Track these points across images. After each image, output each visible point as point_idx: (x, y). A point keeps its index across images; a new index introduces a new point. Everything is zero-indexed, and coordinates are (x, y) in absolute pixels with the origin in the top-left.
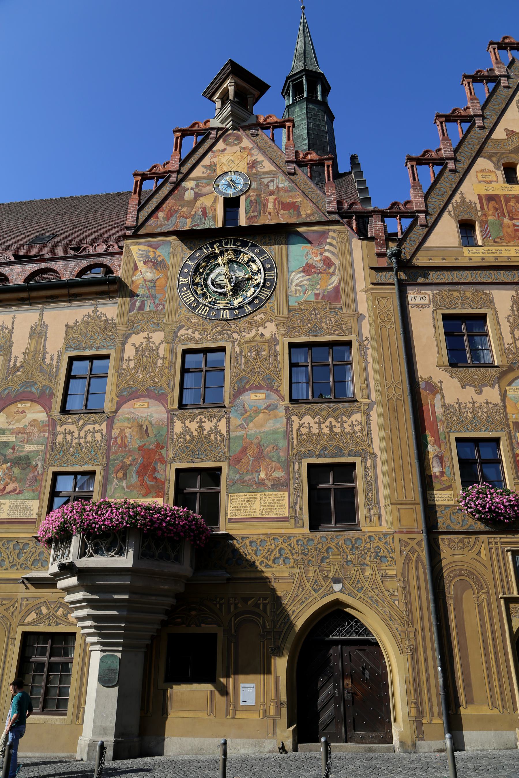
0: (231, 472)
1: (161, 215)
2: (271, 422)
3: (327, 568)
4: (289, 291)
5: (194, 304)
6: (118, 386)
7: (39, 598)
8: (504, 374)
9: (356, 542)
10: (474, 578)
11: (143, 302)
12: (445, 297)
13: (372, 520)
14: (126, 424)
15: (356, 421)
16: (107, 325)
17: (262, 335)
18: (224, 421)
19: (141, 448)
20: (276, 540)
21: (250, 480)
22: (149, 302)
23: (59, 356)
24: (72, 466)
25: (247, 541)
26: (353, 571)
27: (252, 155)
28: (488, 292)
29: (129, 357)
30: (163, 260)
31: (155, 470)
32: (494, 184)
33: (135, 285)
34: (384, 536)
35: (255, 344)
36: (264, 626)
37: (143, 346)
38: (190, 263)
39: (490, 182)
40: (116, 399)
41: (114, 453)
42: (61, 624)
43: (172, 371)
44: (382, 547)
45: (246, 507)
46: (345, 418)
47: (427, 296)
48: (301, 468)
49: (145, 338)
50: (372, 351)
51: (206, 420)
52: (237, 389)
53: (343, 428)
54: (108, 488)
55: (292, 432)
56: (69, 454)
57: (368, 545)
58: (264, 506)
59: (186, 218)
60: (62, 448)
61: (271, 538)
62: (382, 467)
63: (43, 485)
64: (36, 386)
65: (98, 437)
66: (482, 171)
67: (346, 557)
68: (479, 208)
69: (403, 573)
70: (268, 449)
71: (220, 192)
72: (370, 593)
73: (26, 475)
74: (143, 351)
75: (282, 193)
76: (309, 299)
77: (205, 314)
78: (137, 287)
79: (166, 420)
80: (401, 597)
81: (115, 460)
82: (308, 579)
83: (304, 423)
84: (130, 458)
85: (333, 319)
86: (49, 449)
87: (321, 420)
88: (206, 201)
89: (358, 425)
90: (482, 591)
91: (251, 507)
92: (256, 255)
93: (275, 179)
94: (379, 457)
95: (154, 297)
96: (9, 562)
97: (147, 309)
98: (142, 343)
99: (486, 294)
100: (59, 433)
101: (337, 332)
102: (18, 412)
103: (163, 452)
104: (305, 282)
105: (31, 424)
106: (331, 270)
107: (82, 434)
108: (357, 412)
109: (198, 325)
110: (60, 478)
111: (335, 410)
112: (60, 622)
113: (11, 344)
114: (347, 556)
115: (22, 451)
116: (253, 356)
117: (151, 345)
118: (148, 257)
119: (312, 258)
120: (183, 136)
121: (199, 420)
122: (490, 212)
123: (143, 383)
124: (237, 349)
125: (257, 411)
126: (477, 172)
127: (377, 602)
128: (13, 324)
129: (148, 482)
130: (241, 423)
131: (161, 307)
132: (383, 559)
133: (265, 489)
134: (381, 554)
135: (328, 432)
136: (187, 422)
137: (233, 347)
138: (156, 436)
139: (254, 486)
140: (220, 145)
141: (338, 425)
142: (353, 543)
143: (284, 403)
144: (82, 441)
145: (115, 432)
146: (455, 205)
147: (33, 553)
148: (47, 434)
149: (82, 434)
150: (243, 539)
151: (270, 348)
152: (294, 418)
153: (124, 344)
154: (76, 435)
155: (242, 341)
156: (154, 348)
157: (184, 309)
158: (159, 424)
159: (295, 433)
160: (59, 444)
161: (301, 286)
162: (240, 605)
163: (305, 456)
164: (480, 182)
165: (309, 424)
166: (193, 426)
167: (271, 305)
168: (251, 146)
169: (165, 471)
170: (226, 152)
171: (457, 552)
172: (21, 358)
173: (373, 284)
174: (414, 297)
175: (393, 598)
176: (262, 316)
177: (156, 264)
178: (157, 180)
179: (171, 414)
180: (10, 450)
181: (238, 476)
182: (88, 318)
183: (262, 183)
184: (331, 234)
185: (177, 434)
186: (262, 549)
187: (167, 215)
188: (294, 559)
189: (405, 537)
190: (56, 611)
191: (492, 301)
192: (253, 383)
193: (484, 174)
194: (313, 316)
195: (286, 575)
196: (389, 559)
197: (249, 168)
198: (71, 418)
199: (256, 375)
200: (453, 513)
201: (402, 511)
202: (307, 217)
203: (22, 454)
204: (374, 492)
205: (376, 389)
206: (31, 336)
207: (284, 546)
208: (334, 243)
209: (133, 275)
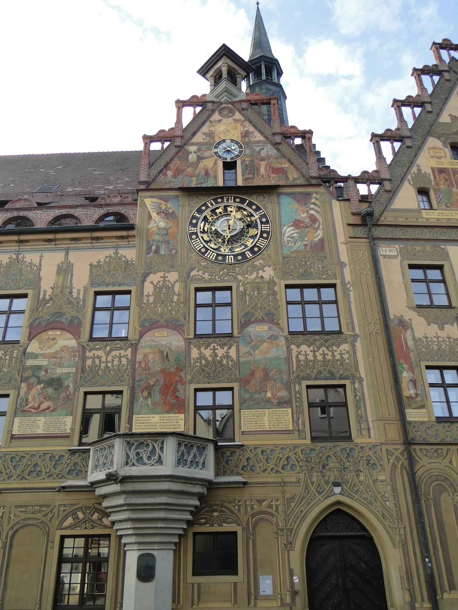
0: (242, 392)
1: (169, 173)
2: (274, 350)
3: (328, 473)
4: (283, 241)
5: (203, 250)
6: (140, 318)
7: (75, 504)
9: (350, 451)
10: (448, 482)
11: (158, 247)
12: (410, 250)
13: (363, 433)
14: (148, 350)
15: (344, 350)
17: (262, 277)
18: (234, 348)
19: (162, 371)
20: (283, 449)
21: (258, 398)
22: (163, 247)
23: (85, 291)
24: (101, 386)
25: (259, 451)
26: (349, 476)
27: (244, 126)
28: (443, 247)
29: (148, 293)
30: (174, 211)
31: (176, 390)
32: (443, 160)
33: (150, 232)
34: (373, 446)
36: (277, 525)
37: (161, 284)
38: (197, 215)
39: (440, 158)
41: (138, 375)
42: (96, 527)
43: (187, 306)
44: (372, 456)
45: (257, 421)
46: (335, 348)
47: (395, 249)
48: (301, 389)
49: (162, 277)
50: (354, 293)
51: (219, 347)
52: (243, 322)
53: (334, 356)
54: (135, 405)
55: (292, 358)
56: (98, 376)
57: (361, 454)
58: (272, 421)
59: (192, 177)
60: (91, 371)
61: (279, 448)
62: (368, 389)
63: (75, 403)
64: (65, 317)
65: (124, 361)
66: (434, 148)
67: (342, 464)
68: (432, 178)
69: (391, 478)
70: (273, 372)
71: (220, 157)
72: (365, 495)
73: (59, 395)
74: (161, 288)
75: (271, 160)
76: (299, 249)
77: (213, 259)
78: (152, 233)
79: (184, 347)
80: (391, 498)
81: (140, 381)
82: (312, 483)
83: (301, 351)
84: (153, 380)
85: (320, 266)
86: (80, 371)
87: (316, 349)
88: (209, 163)
89: (346, 353)
90: (456, 494)
91: (260, 421)
92: (253, 210)
93: (265, 147)
94: (365, 380)
95: (168, 243)
96: (46, 473)
97: (162, 253)
98: (159, 282)
99: (442, 249)
100: (88, 358)
101: (324, 276)
102: (49, 339)
103: (183, 374)
105: (62, 350)
106: (316, 225)
107: (110, 358)
108: (345, 343)
109: (208, 268)
110: (89, 397)
111: (326, 341)
112: (95, 525)
113: (40, 279)
114: (344, 463)
115: (54, 374)
116: (256, 294)
117: (168, 283)
118: (160, 208)
119: (300, 215)
120: (183, 106)
121: (212, 348)
122: (442, 182)
123: (162, 315)
124: (241, 289)
125: (262, 341)
126: (429, 149)
127: (371, 503)
128: (40, 262)
129: (170, 400)
130: (248, 350)
131: (174, 251)
132: (374, 466)
133: (272, 406)
134: (372, 462)
135: (322, 359)
136: (202, 349)
137: (238, 287)
138: (175, 360)
139: (262, 404)
140: (216, 116)
141: (330, 353)
142: (348, 452)
143: (284, 334)
144: (109, 365)
145: (139, 357)
146: (413, 175)
147: (68, 464)
149: (110, 358)
150: (255, 449)
151: (269, 289)
152: (293, 347)
153: (143, 282)
154: (104, 359)
155: (246, 282)
156: (170, 286)
157: (195, 254)
158: (178, 351)
159: (294, 359)
160: (89, 367)
161: (292, 238)
162: (255, 506)
163: (304, 378)
164: (432, 157)
165: (306, 352)
166: (207, 353)
167: (268, 253)
168: (243, 119)
169: (185, 390)
170: (222, 122)
171: (433, 461)
172: (49, 292)
173: (350, 237)
174: (384, 250)
175: (385, 499)
176: (261, 261)
177: (167, 215)
178: (163, 144)
179: (188, 341)
180: (43, 373)
181: (248, 395)
182: (110, 259)
183: (254, 150)
184: (314, 195)
185: (194, 359)
186: (272, 457)
187: (174, 174)
188: (301, 466)
189: (391, 448)
190: (92, 516)
191: (447, 255)
193: (435, 151)
194: (303, 263)
195: (294, 480)
196: (379, 466)
197: (242, 137)
198: (99, 345)
199: (259, 311)
200: (428, 428)
201: (386, 425)
202: (293, 181)
203: (55, 376)
204: (363, 409)
205: (359, 325)
206: (58, 273)
207: (291, 454)
208: (318, 203)
209: (148, 223)
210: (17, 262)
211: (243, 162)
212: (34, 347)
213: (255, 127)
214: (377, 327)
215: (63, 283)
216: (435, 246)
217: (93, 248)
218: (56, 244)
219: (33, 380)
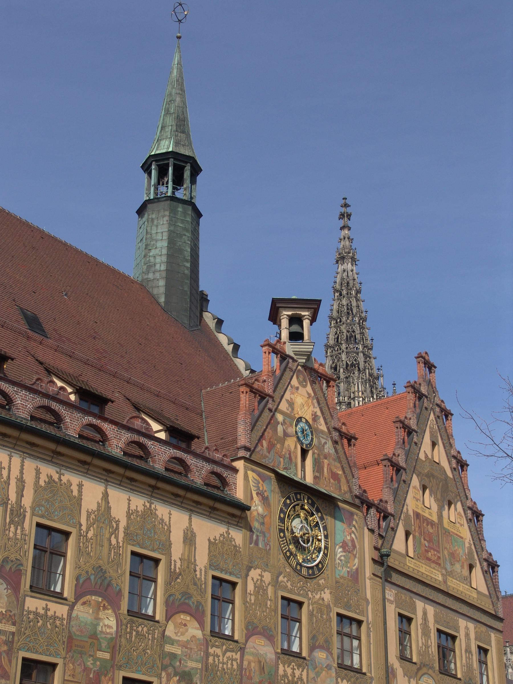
6: (245, 619)
8: (419, 669)
17: (323, 599)
35: (319, 607)
40: (245, 631)
59: (280, 457)
86: (204, 669)
97: (260, 546)
104: (342, 558)
124: (311, 608)
125: (322, 669)
128: (170, 521)
144: (225, 666)
145: (245, 663)
148: (202, 653)
149: (225, 660)
153: (247, 575)
154: (221, 658)
168: (313, 395)
177: (265, 500)
180: (178, 663)
184: (355, 517)
192: (320, 643)
198: (218, 642)
203: (187, 669)
206: (184, 542)
208: (356, 526)
210: (149, 514)
211: (314, 453)
212: (170, 631)
214: (383, 673)
215: (188, 556)
216: (411, 598)
218: (182, 503)
219: (170, 670)
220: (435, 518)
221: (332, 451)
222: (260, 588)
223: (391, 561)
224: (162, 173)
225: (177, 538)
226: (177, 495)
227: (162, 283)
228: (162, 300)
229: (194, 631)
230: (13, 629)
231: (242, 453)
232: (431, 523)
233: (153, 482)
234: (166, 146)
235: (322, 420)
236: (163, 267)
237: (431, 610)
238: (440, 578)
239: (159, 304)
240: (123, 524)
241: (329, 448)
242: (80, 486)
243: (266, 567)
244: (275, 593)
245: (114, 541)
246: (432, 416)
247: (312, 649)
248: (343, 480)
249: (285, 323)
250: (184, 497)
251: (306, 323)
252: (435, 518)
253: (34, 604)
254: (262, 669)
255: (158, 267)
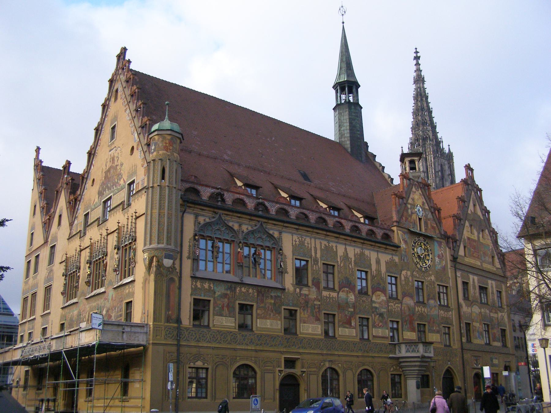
16: (396, 265)
172: (375, 272)
177: (406, 242)
210: (362, 254)
212: (374, 298)
213: (426, 201)
214: (457, 306)
217: (385, 253)
219: (375, 313)
220: (476, 238)
221: (431, 217)
222: (406, 278)
223: (458, 260)
224: (343, 90)
225: (373, 262)
226: (372, 245)
227: (348, 142)
228: (349, 150)
229: (383, 298)
230: (319, 303)
231: (395, 224)
232: (474, 241)
233: (362, 241)
234: (344, 78)
235: (426, 204)
236: (348, 135)
237: (476, 278)
238: (480, 264)
239: (348, 152)
240: (353, 260)
241: (430, 216)
242: (336, 247)
243: (408, 269)
244: (412, 280)
245: (350, 267)
246: (473, 193)
247: (428, 300)
248: (436, 228)
249: (407, 163)
250: (375, 246)
251: (416, 163)
252: (476, 238)
253: (325, 293)
254: (409, 310)
255: (346, 135)
